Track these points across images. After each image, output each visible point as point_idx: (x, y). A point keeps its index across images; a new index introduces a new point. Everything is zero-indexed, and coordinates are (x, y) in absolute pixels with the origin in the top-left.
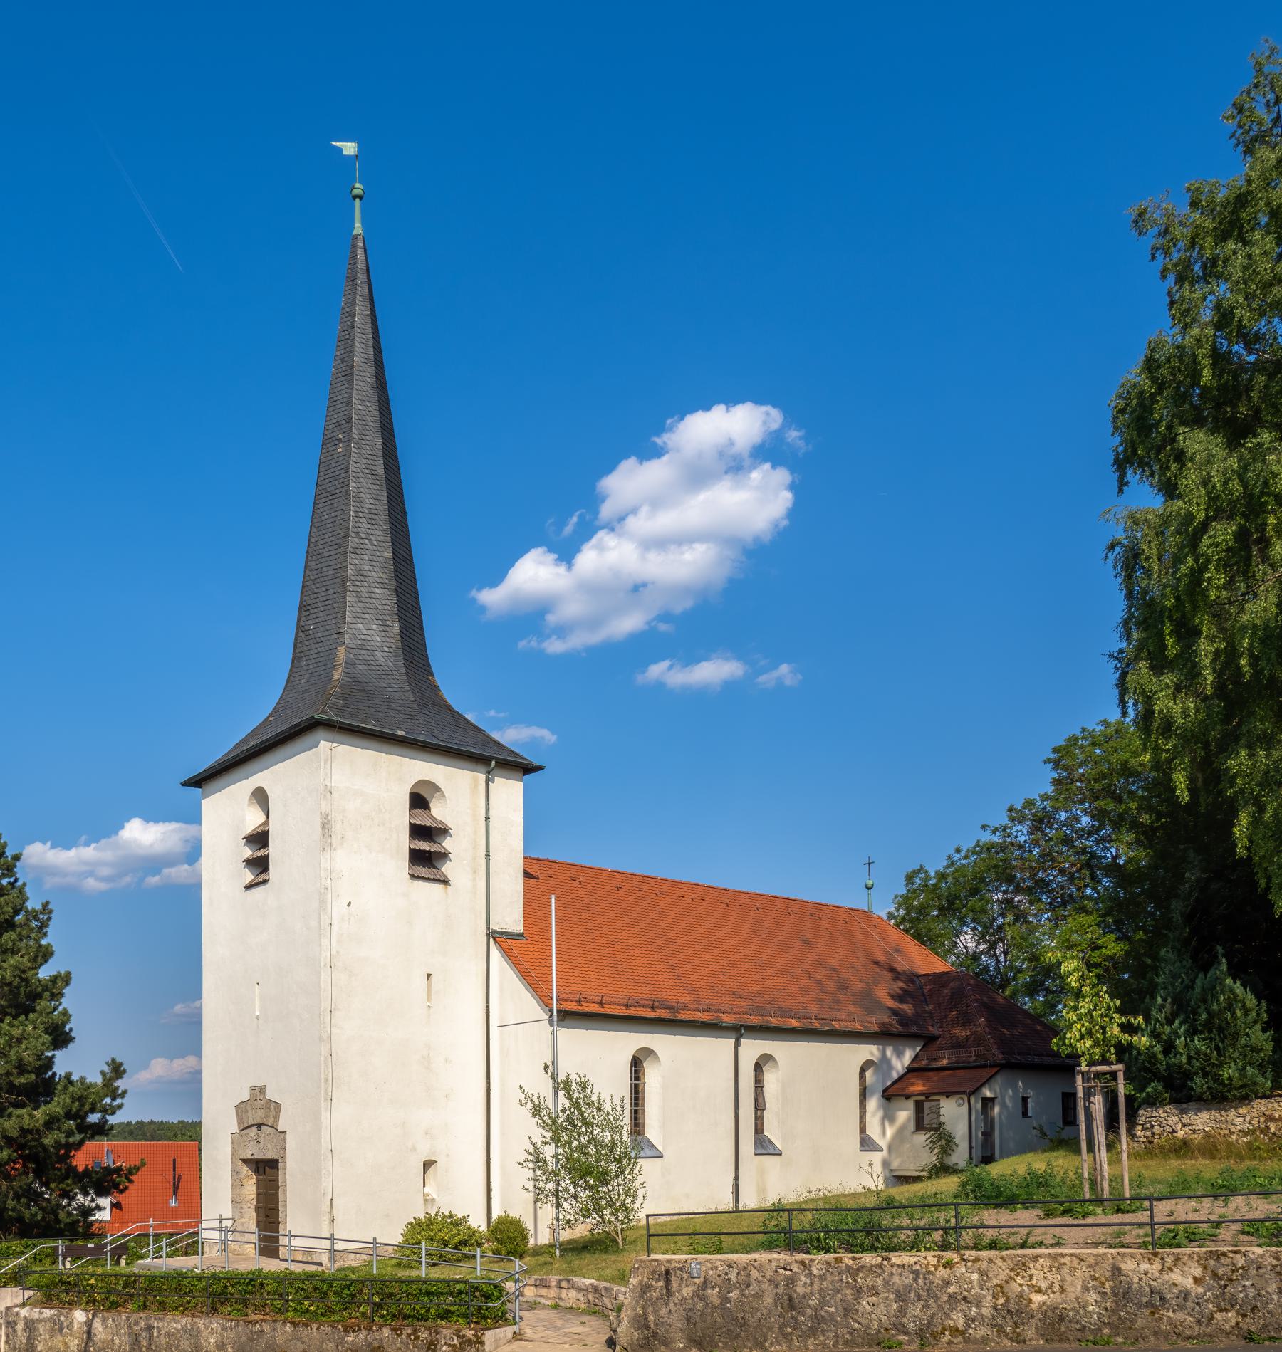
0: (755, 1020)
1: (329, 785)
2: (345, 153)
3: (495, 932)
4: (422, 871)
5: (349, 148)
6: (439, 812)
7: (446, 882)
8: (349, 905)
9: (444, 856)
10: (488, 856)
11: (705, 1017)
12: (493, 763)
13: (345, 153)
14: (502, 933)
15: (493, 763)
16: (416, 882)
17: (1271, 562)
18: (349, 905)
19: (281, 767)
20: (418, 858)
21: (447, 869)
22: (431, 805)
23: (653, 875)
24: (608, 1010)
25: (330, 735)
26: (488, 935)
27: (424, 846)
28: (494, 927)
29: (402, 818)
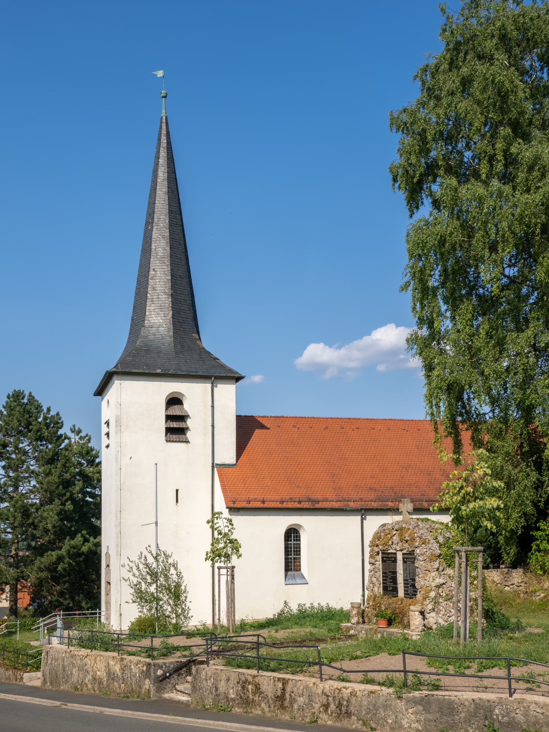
0: (375, 505)
1: (119, 401)
2: (158, 76)
3: (217, 465)
4: (174, 437)
5: (160, 74)
6: (188, 406)
7: (187, 442)
8: (131, 458)
9: (187, 428)
10: (213, 426)
11: (336, 505)
12: (213, 378)
13: (158, 76)
14: (222, 465)
15: (213, 378)
16: (169, 444)
17: (514, 184)
18: (131, 458)
19: (108, 393)
20: (169, 431)
21: (189, 435)
22: (184, 402)
23: (357, 417)
24: (266, 505)
25: (119, 377)
26: (213, 467)
27: (174, 425)
28: (217, 461)
29: (161, 412)
